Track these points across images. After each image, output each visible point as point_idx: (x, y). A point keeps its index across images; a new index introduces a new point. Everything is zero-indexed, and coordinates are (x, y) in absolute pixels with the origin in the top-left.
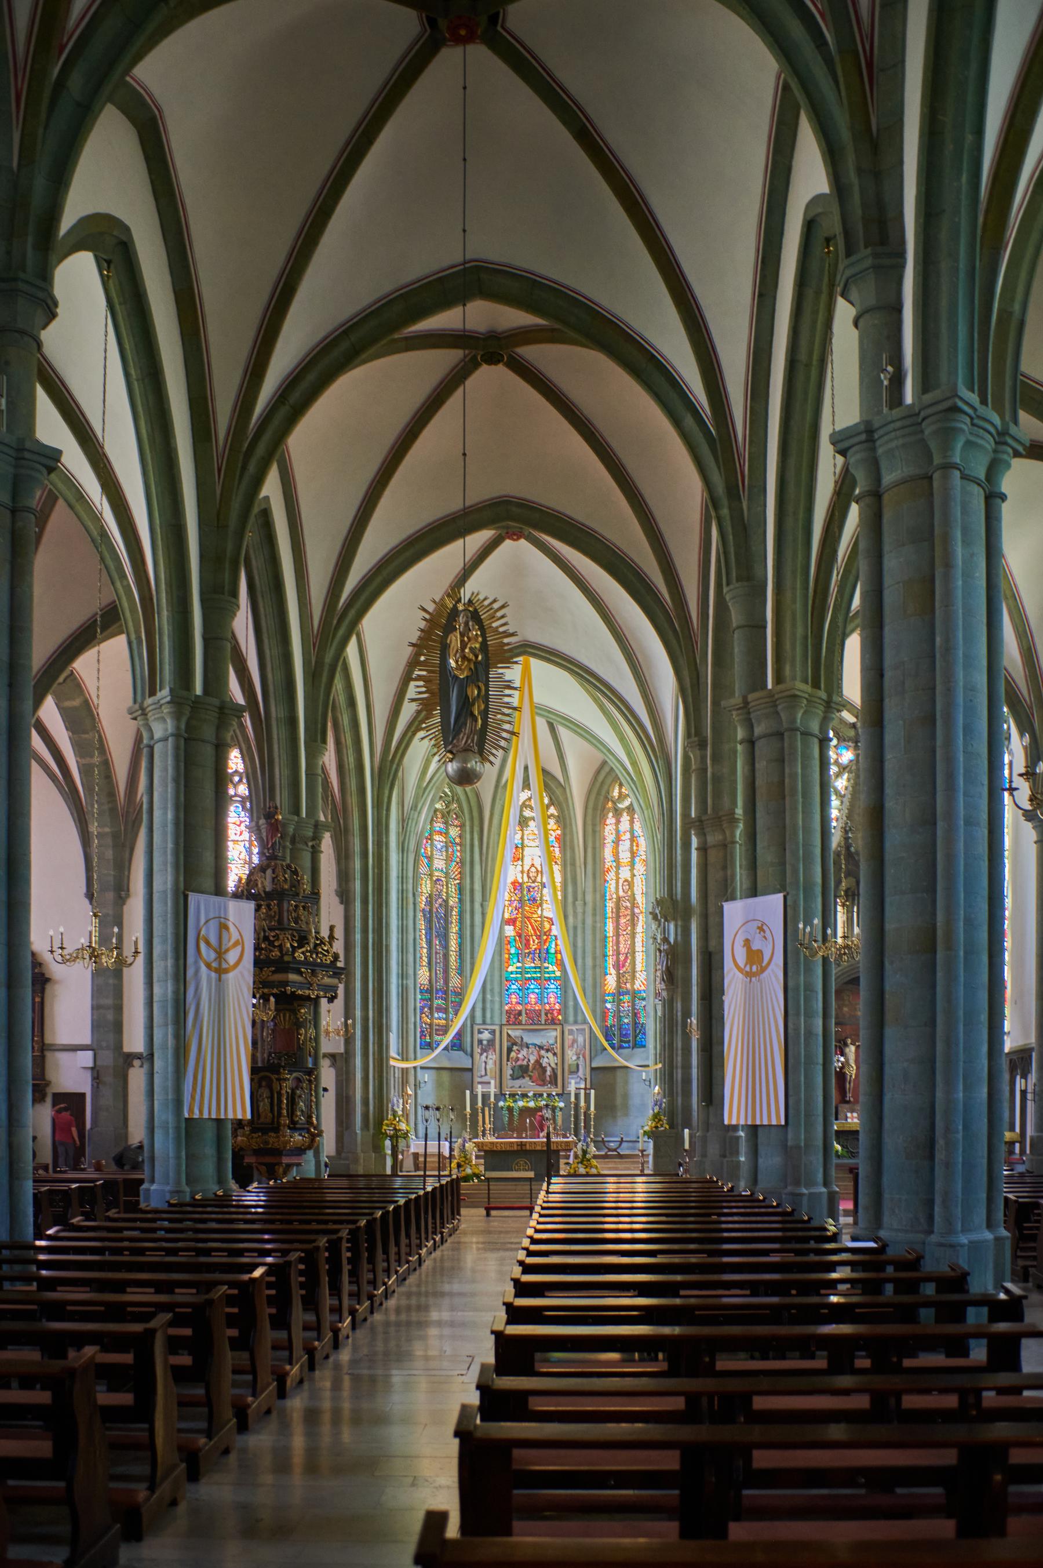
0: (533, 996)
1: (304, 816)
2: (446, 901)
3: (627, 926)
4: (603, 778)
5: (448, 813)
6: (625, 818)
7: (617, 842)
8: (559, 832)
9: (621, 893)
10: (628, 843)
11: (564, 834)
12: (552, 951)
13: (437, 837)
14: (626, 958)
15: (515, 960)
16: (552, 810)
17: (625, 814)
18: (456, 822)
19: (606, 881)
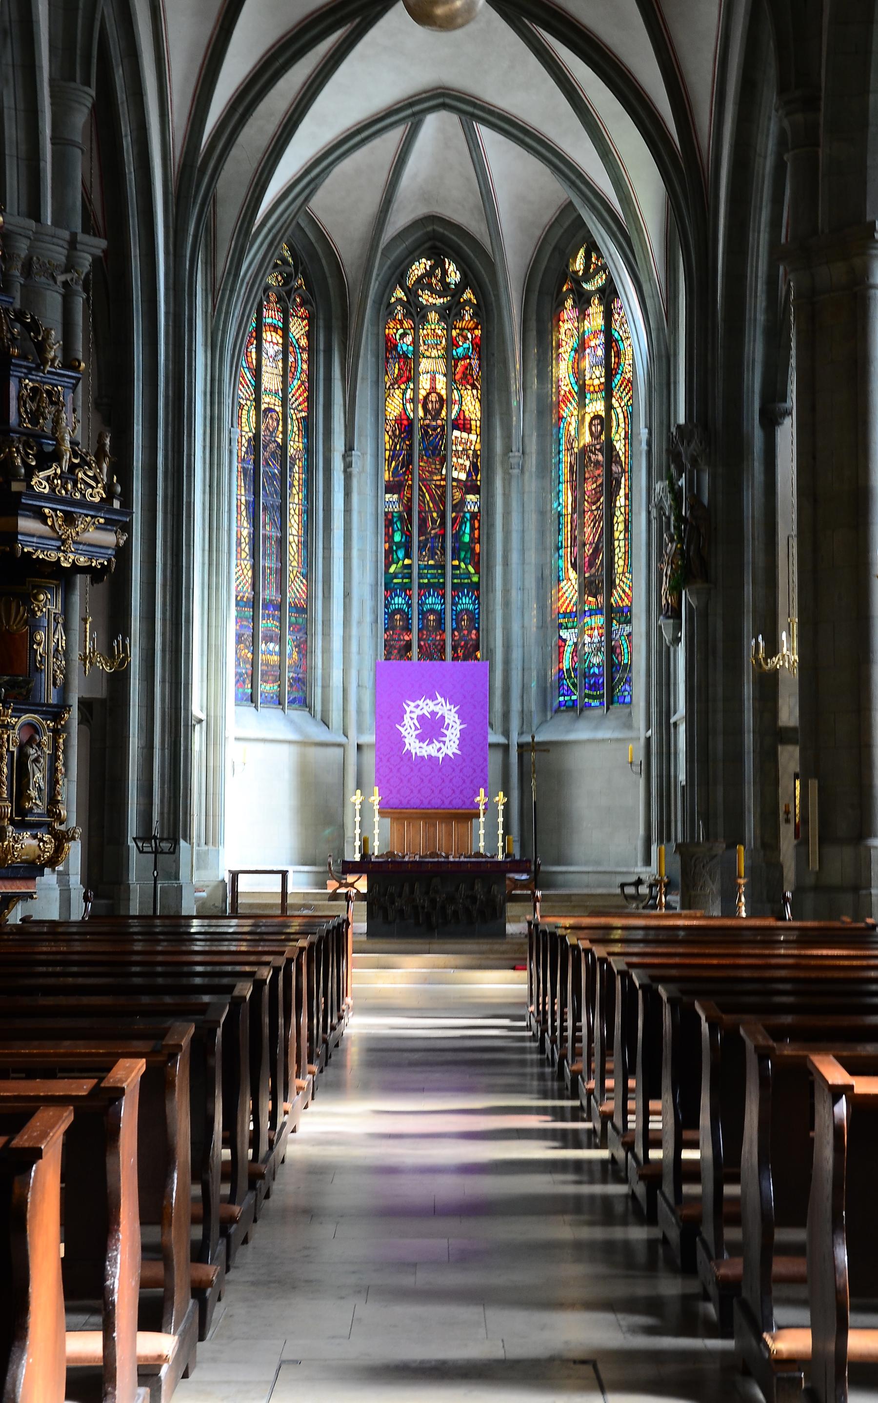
0: (432, 617)
2: (284, 447)
3: (597, 493)
4: (564, 236)
5: (288, 294)
6: (596, 310)
7: (581, 348)
12: (467, 539)
15: (401, 554)
16: (468, 295)
19: (561, 418)
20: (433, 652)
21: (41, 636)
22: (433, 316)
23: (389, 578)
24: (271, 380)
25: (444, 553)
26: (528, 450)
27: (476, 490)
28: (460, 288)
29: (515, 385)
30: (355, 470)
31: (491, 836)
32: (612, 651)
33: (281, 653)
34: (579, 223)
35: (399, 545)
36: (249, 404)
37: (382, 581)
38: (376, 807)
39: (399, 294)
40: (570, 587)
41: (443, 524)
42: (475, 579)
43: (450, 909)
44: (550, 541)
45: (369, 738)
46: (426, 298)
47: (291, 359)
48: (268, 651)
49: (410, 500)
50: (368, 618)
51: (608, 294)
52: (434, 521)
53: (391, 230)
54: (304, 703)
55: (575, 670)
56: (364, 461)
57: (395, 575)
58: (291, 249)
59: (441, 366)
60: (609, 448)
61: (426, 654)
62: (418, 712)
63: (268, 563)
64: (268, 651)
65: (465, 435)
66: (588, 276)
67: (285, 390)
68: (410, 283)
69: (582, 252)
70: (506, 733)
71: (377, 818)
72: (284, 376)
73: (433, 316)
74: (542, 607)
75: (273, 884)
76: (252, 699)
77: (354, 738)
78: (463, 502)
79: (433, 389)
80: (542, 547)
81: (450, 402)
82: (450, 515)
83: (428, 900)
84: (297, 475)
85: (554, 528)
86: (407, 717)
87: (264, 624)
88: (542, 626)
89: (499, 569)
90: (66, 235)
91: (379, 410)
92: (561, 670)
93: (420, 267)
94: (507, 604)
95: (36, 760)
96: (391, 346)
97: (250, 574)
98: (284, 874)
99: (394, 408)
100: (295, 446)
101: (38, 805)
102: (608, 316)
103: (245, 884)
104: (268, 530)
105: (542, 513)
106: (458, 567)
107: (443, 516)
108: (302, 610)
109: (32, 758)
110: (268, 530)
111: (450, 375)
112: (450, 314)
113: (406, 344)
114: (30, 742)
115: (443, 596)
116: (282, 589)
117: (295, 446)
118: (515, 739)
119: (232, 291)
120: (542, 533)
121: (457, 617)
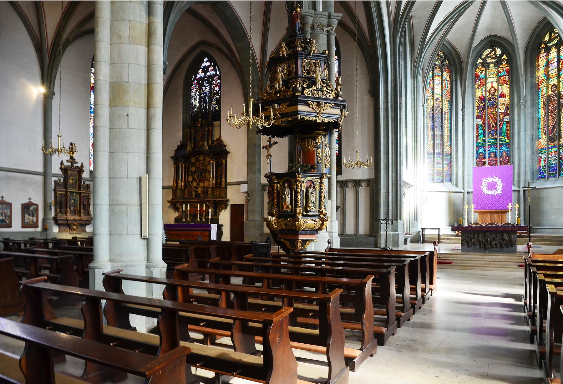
1: (321, 10)
2: (442, 109)
5: (443, 66)
8: (508, 68)
9: (550, 93)
10: (556, 64)
11: (511, 68)
12: (504, 130)
14: (554, 128)
15: (482, 136)
16: (504, 57)
17: (554, 48)
18: (447, 70)
19: (539, 88)
21: (319, 151)
22: (492, 65)
25: (497, 135)
26: (527, 100)
27: (508, 115)
28: (501, 55)
31: (513, 217)
33: (442, 167)
35: (481, 134)
36: (431, 98)
38: (473, 210)
39: (480, 61)
40: (544, 141)
41: (496, 126)
42: (508, 141)
43: (494, 243)
46: (489, 60)
47: (444, 84)
49: (485, 120)
50: (471, 155)
52: (493, 126)
54: (451, 181)
55: (545, 166)
57: (480, 143)
59: (495, 79)
62: (487, 181)
65: (504, 99)
68: (483, 57)
70: (519, 187)
71: (473, 212)
72: (442, 89)
73: (492, 65)
74: (532, 148)
75: (436, 232)
77: (467, 190)
78: (503, 119)
79: (492, 87)
80: (533, 129)
81: (498, 90)
82: (499, 123)
83: (484, 238)
84: (447, 117)
86: (483, 183)
88: (532, 153)
90: (327, 14)
91: (473, 95)
92: (540, 166)
94: (519, 148)
95: (312, 193)
96: (477, 76)
98: (439, 229)
99: (479, 93)
101: (313, 210)
103: (426, 232)
105: (533, 119)
106: (502, 138)
107: (496, 124)
109: (310, 192)
111: (498, 82)
113: (482, 75)
114: (310, 187)
115: (496, 147)
117: (446, 108)
119: (420, 61)
120: (533, 125)
121: (501, 154)
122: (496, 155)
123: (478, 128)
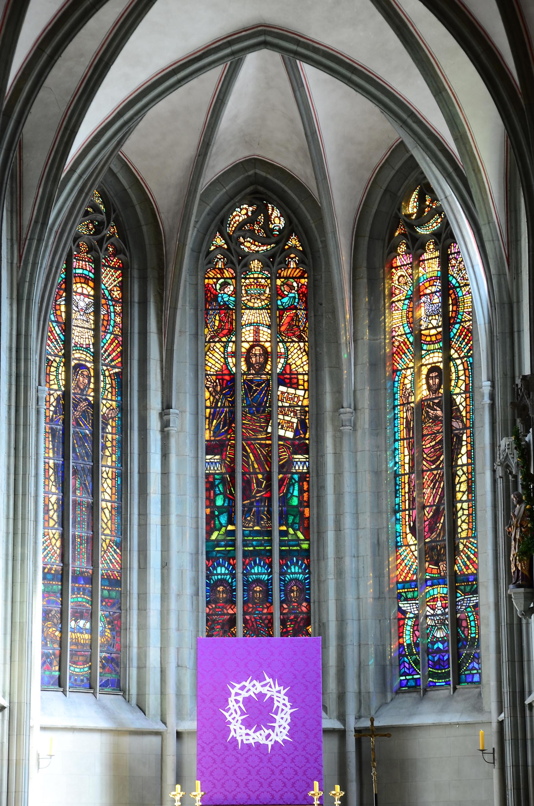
0: (258, 589)
2: (95, 406)
5: (100, 242)
12: (295, 502)
13: (77, 287)
15: (223, 519)
16: (293, 241)
19: (395, 371)
20: (260, 627)
22: (255, 265)
23: (211, 545)
24: (82, 335)
27: (304, 449)
29: (345, 336)
30: (173, 429)
32: (457, 623)
33: (93, 631)
34: (412, 164)
37: (203, 549)
39: (219, 241)
40: (409, 554)
41: (269, 486)
42: (305, 546)
44: (387, 503)
45: (190, 725)
46: (248, 246)
47: (103, 312)
48: (78, 629)
49: (233, 460)
50: (188, 590)
51: (445, 238)
52: (259, 483)
53: (210, 175)
54: (118, 686)
56: (183, 420)
57: (217, 543)
58: (103, 195)
59: (264, 317)
60: (449, 402)
61: (251, 629)
63: (78, 531)
64: (78, 629)
66: (422, 219)
67: (96, 344)
69: (415, 195)
72: (96, 330)
73: (255, 265)
74: (379, 576)
76: (60, 683)
77: (173, 725)
78: (290, 463)
79: (256, 343)
80: (377, 510)
82: (276, 477)
84: (110, 435)
85: (390, 489)
86: (231, 700)
87: (74, 599)
88: (379, 597)
89: (330, 535)
91: (198, 365)
92: (401, 645)
93: (241, 214)
94: (340, 573)
96: (210, 296)
97: (58, 544)
99: (214, 362)
100: (108, 405)
102: (445, 261)
104: (78, 495)
105: (377, 473)
107: (269, 478)
108: (116, 582)
110: (78, 495)
112: (273, 262)
115: (270, 566)
116: (93, 560)
117: (108, 405)
118: (352, 724)
120: (377, 495)
121: (286, 588)
122: (268, 593)
123: (210, 486)
